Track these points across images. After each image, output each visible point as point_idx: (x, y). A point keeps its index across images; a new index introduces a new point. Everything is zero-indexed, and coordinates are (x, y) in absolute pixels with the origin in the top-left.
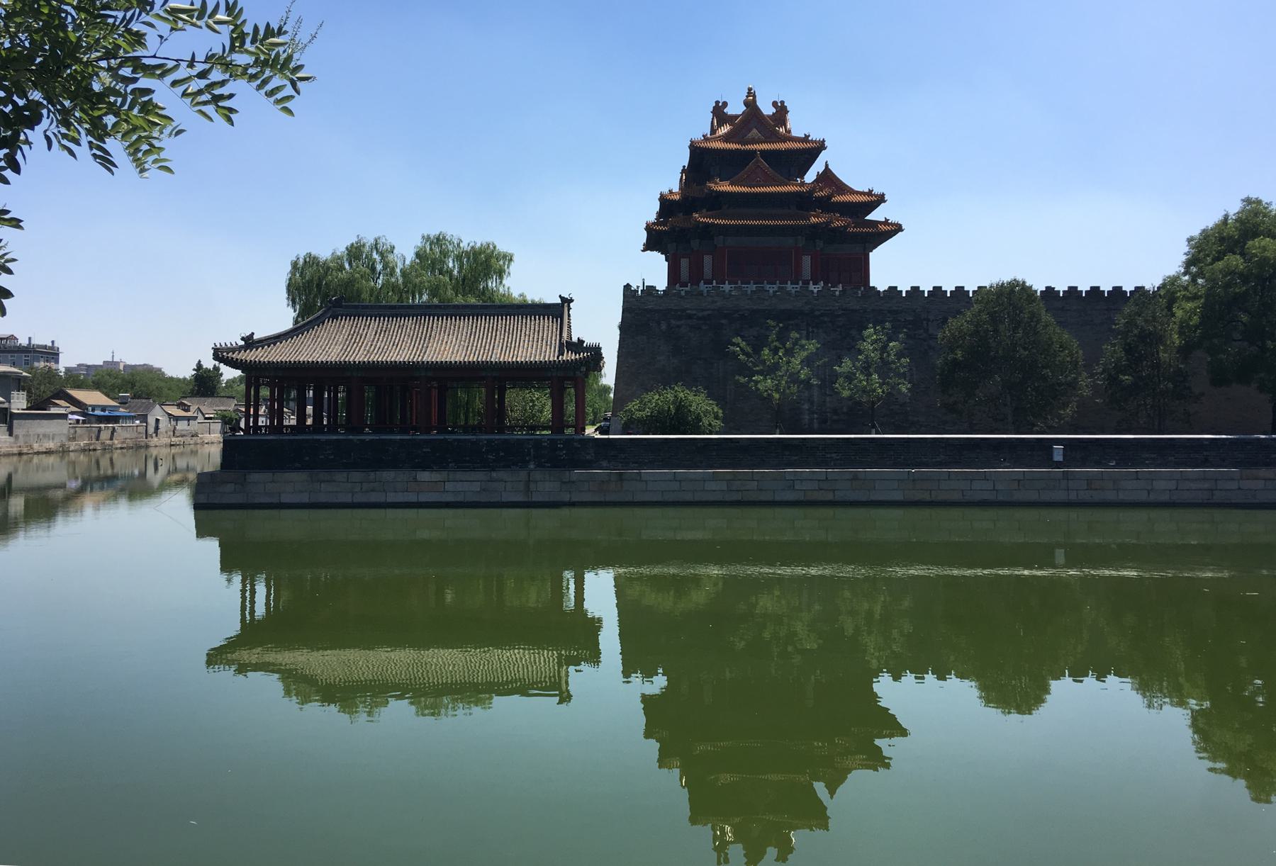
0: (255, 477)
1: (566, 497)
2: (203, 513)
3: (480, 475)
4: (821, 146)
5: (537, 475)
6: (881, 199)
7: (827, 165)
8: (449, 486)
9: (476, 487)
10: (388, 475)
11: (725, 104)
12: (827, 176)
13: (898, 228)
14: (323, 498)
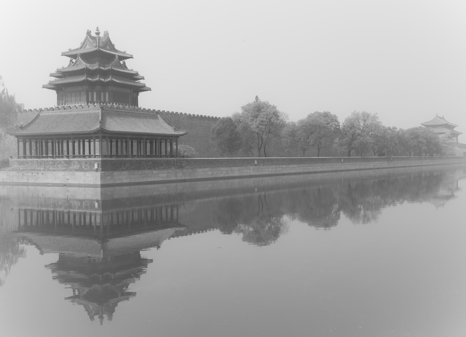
0: (116, 173)
1: (183, 178)
2: (103, 189)
3: (166, 171)
4: (132, 58)
5: (178, 171)
6: (143, 78)
7: (124, 63)
8: (160, 175)
9: (165, 175)
10: (147, 171)
11: (90, 31)
12: (124, 66)
14: (132, 181)
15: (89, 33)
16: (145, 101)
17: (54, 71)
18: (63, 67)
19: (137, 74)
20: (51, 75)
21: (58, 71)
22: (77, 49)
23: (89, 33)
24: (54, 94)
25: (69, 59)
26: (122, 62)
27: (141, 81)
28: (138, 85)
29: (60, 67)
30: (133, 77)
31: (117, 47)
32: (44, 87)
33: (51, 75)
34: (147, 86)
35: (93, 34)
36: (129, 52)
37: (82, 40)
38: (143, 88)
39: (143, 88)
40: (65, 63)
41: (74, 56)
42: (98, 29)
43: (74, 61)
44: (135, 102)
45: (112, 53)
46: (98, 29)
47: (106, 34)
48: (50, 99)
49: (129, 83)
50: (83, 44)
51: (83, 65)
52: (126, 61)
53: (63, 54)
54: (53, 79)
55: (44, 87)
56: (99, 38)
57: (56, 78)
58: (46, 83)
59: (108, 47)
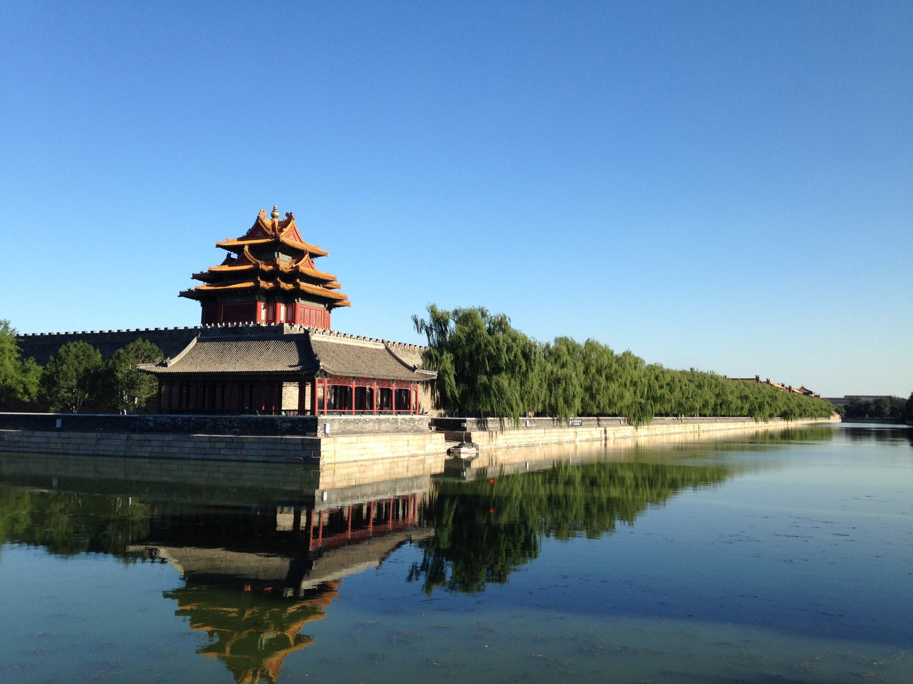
20: (195, 277)
21: (211, 273)
22: (240, 239)
25: (226, 252)
32: (182, 294)
33: (195, 277)
37: (251, 225)
41: (238, 249)
43: (234, 256)
45: (297, 244)
48: (190, 315)
50: (251, 234)
52: (315, 260)
53: (218, 246)
54: (201, 285)
55: (182, 294)
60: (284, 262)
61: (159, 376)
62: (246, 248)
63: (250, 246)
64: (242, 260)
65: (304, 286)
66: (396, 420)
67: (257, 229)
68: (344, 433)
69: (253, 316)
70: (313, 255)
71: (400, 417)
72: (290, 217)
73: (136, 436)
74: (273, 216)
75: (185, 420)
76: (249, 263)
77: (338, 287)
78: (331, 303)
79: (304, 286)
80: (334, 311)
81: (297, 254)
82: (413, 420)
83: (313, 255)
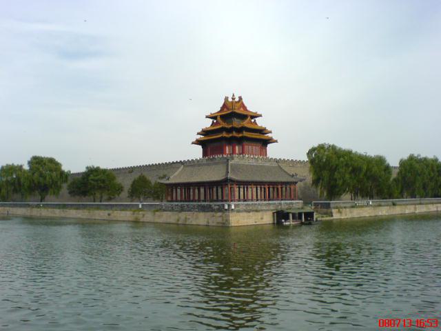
4: (261, 116)
6: (271, 132)
13: (276, 141)
15: (226, 99)
16: (272, 151)
17: (200, 131)
18: (13, 164)
19: (265, 129)
20: (198, 134)
21: (203, 131)
22: (218, 112)
23: (226, 99)
24: (199, 149)
25: (211, 120)
26: (253, 120)
27: (270, 135)
28: (267, 138)
29: (204, 127)
30: (262, 131)
31: (248, 109)
32: (193, 143)
33: (198, 134)
34: (275, 138)
35: (230, 100)
36: (259, 113)
37: (221, 105)
38: (269, 141)
39: (269, 141)
40: (208, 124)
42: (233, 96)
44: (263, 151)
45: (245, 113)
46: (233, 96)
47: (240, 98)
48: (197, 153)
49: (258, 137)
50: (222, 109)
51: (223, 125)
52: (257, 119)
53: (207, 117)
55: (193, 143)
56: (236, 102)
57: (202, 136)
58: (194, 140)
59: (242, 109)
60: (236, 123)
61: (167, 185)
62: (219, 118)
63: (221, 116)
64: (217, 123)
65: (246, 134)
66: (280, 204)
67: (224, 106)
68: (246, 211)
69: (222, 151)
70: (253, 117)
71: (282, 202)
72: (240, 98)
73: (157, 213)
74: (233, 99)
75: (176, 205)
76: (220, 124)
77: (271, 132)
78: (266, 142)
79: (246, 134)
80: (269, 146)
81: (243, 117)
82: (292, 204)
83: (253, 117)
